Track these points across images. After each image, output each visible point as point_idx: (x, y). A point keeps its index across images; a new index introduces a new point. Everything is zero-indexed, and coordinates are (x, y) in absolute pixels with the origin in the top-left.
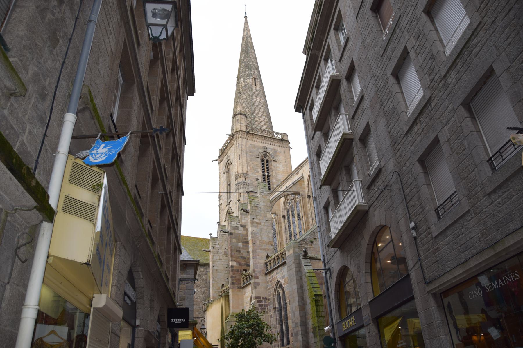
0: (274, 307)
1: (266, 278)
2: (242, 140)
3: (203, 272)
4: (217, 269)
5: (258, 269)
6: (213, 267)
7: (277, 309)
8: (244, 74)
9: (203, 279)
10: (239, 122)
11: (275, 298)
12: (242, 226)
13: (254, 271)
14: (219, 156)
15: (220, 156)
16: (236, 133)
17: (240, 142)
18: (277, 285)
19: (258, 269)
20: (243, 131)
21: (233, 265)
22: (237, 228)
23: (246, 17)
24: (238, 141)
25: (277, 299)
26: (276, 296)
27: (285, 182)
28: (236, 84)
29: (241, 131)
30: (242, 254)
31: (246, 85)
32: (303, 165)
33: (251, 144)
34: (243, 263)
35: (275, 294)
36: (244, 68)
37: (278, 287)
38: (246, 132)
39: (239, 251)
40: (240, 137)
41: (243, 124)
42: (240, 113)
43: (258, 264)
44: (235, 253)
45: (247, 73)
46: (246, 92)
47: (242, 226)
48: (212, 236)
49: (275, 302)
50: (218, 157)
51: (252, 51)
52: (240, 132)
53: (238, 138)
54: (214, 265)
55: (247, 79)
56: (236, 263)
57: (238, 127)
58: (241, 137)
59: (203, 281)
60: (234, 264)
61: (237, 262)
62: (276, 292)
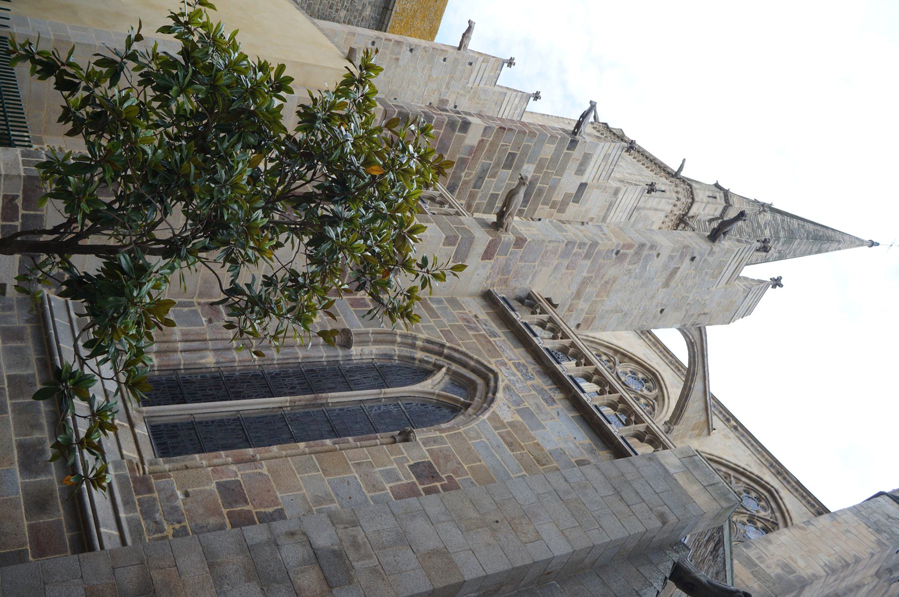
0: (354, 338)
1: (472, 295)
2: (670, 201)
3: (360, 14)
4: (401, 63)
5: (522, 259)
6: (411, 50)
7: (340, 352)
8: (778, 226)
9: (337, 11)
10: (711, 199)
11: (393, 342)
12: (583, 186)
13: (520, 242)
14: (610, 126)
15: (611, 131)
16: (688, 187)
17: (668, 194)
18: (465, 365)
19: (522, 259)
20: (689, 208)
21: (472, 130)
22: (580, 171)
23: (872, 244)
24: (670, 191)
25: (390, 357)
26: (406, 352)
27: (661, 352)
28: (759, 200)
29: (692, 204)
30: (493, 176)
31: (759, 226)
32: (743, 436)
33: (653, 223)
34: (463, 174)
35: (413, 346)
36: (789, 226)
37: (455, 367)
38: (686, 214)
39: (507, 166)
40: (680, 196)
41: (704, 210)
42: (731, 205)
43: (536, 264)
44: (508, 144)
45: (782, 234)
46: (747, 227)
47: (583, 186)
48: (506, 65)
49: (376, 342)
50: (606, 124)
51: (815, 249)
52: (690, 200)
53: (676, 189)
54: (418, 53)
55: (770, 232)
56: (472, 147)
57: (700, 195)
58: (678, 199)
59: (331, 8)
60: (472, 138)
61: (474, 151)
62: (424, 349)
